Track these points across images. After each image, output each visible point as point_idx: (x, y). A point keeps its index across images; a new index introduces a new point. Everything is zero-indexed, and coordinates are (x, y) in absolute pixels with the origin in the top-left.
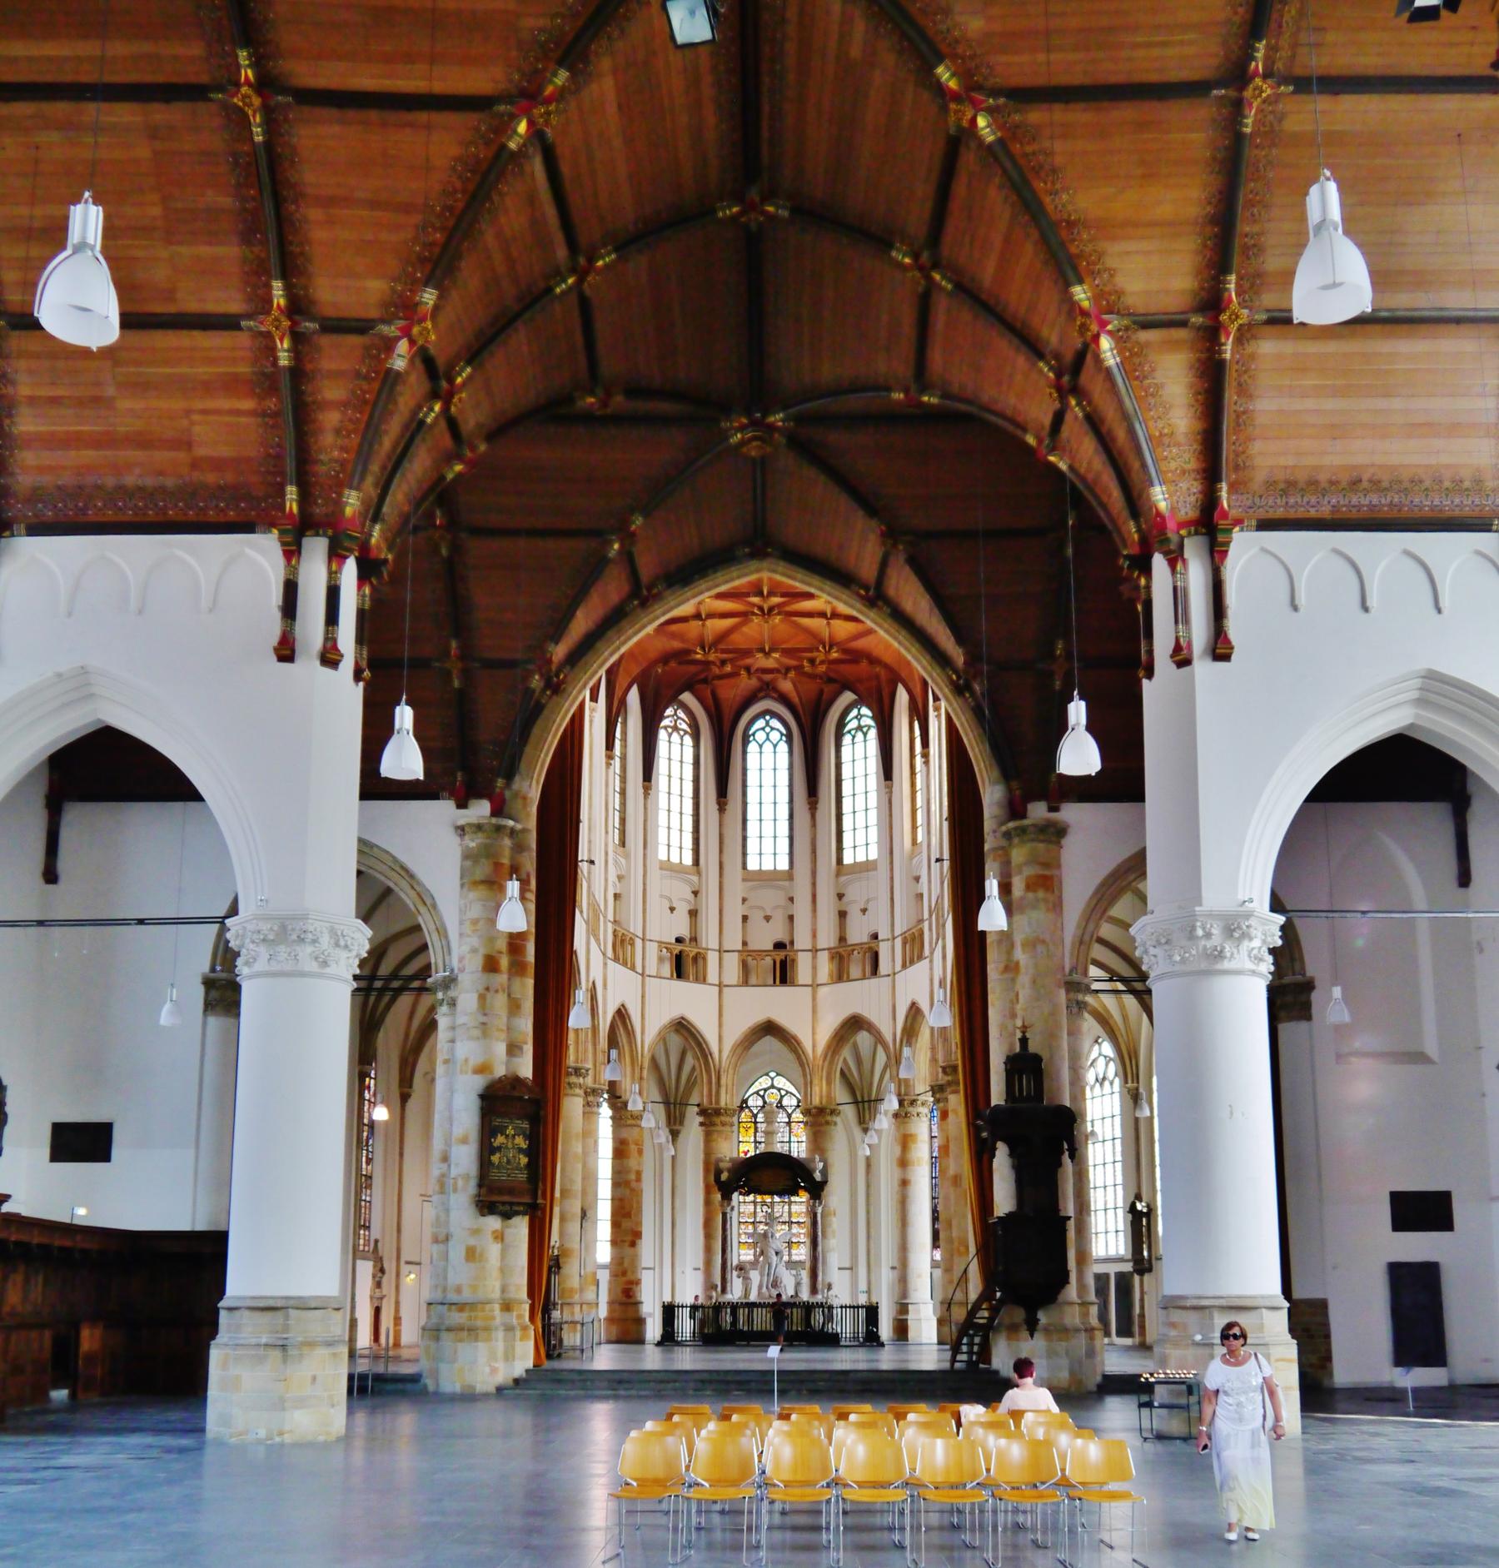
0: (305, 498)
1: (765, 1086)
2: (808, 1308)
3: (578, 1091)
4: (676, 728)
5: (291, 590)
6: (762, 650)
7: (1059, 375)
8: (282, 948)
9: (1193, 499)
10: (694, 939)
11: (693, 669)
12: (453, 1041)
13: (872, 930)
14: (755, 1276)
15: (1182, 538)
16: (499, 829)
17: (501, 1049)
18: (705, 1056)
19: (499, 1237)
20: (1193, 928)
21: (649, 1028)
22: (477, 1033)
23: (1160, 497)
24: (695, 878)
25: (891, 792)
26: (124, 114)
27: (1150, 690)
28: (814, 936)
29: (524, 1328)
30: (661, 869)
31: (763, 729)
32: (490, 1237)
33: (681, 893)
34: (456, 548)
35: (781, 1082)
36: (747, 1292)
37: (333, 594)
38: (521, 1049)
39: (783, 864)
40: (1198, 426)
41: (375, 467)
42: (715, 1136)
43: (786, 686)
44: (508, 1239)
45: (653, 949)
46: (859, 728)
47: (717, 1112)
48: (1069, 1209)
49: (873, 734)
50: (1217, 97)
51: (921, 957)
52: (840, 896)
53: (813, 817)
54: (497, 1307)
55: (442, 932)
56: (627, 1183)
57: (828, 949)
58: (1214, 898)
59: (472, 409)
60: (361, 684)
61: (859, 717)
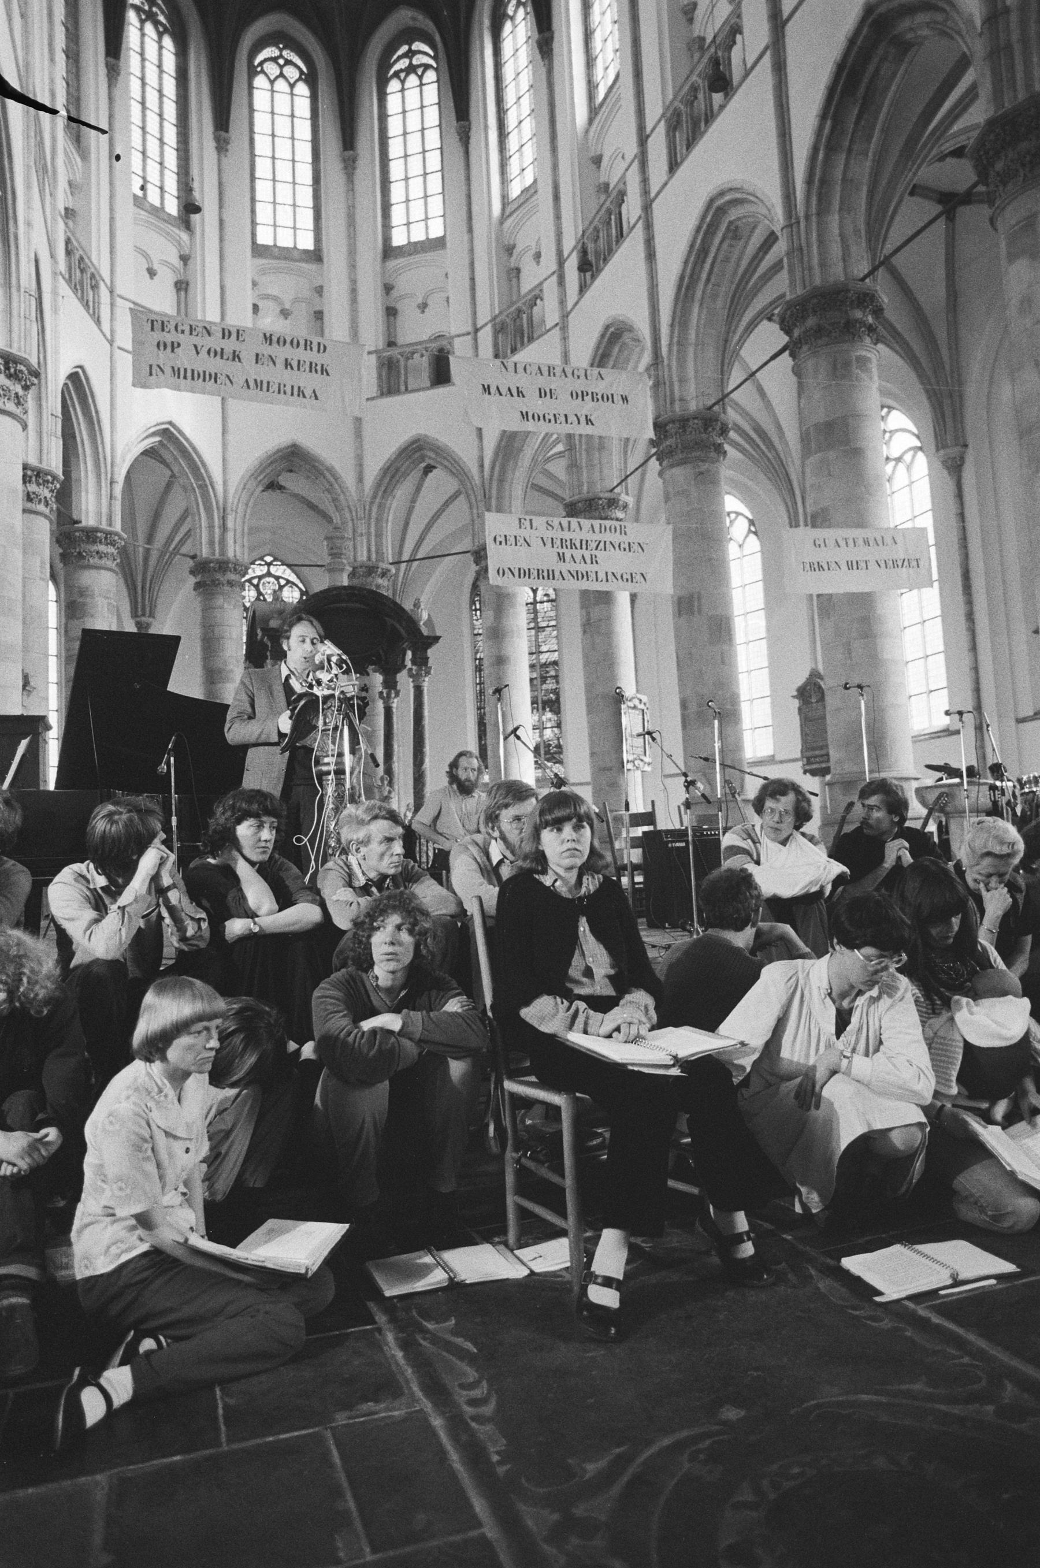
1: (259, 573)
18: (203, 487)
24: (184, 236)
25: (465, 138)
31: (274, 60)
35: (278, 570)
39: (306, 242)
42: (220, 601)
47: (223, 565)
49: (431, 76)
52: (388, 288)
57: (376, 352)
61: (410, 54)
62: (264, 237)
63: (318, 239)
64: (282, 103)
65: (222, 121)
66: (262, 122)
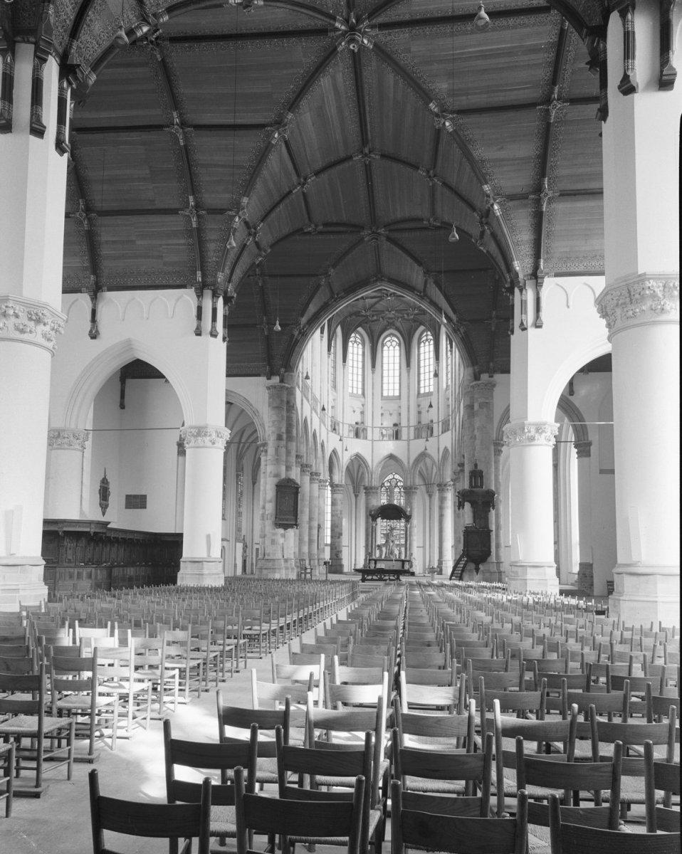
0: (203, 276)
2: (403, 562)
3: (316, 481)
4: (355, 342)
5: (200, 309)
6: (388, 310)
7: (481, 218)
8: (199, 438)
9: (529, 266)
10: (363, 423)
12: (266, 465)
13: (430, 419)
14: (384, 549)
15: (525, 281)
16: (282, 387)
17: (283, 468)
19: (283, 536)
20: (524, 429)
21: (345, 459)
22: (275, 462)
23: (517, 266)
24: (363, 400)
27: (513, 338)
28: (409, 421)
29: (292, 569)
30: (350, 396)
32: (279, 536)
33: (357, 405)
35: (397, 477)
36: (381, 555)
37: (214, 311)
38: (291, 468)
39: (397, 393)
40: (532, 237)
41: (228, 263)
42: (370, 497)
43: (398, 324)
44: (286, 537)
45: (346, 427)
46: (427, 340)
47: (371, 488)
48: (493, 527)
49: (432, 342)
50: (539, 109)
51: (448, 430)
52: (419, 406)
53: (409, 375)
54: (283, 561)
55: (263, 425)
56: (337, 515)
58: (532, 417)
59: (265, 236)
60: (226, 343)
61: (427, 335)
62: (385, 394)
63: (400, 393)
64: (391, 353)
65: (373, 366)
66: (385, 360)
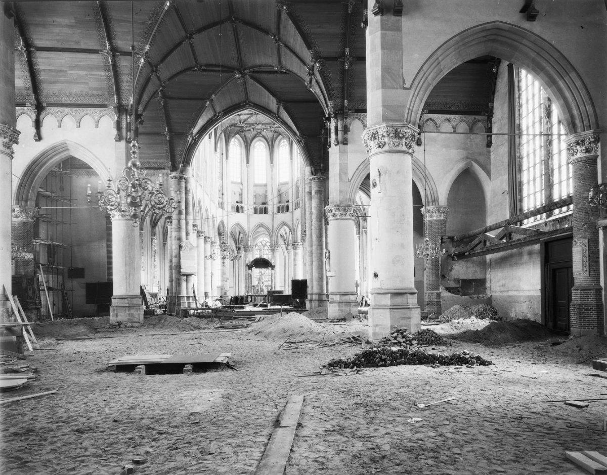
11: (239, 128)
12: (172, 232)
24: (241, 186)
26: (64, 101)
33: (237, 190)
34: (165, 103)
54: (186, 298)
65: (248, 162)
